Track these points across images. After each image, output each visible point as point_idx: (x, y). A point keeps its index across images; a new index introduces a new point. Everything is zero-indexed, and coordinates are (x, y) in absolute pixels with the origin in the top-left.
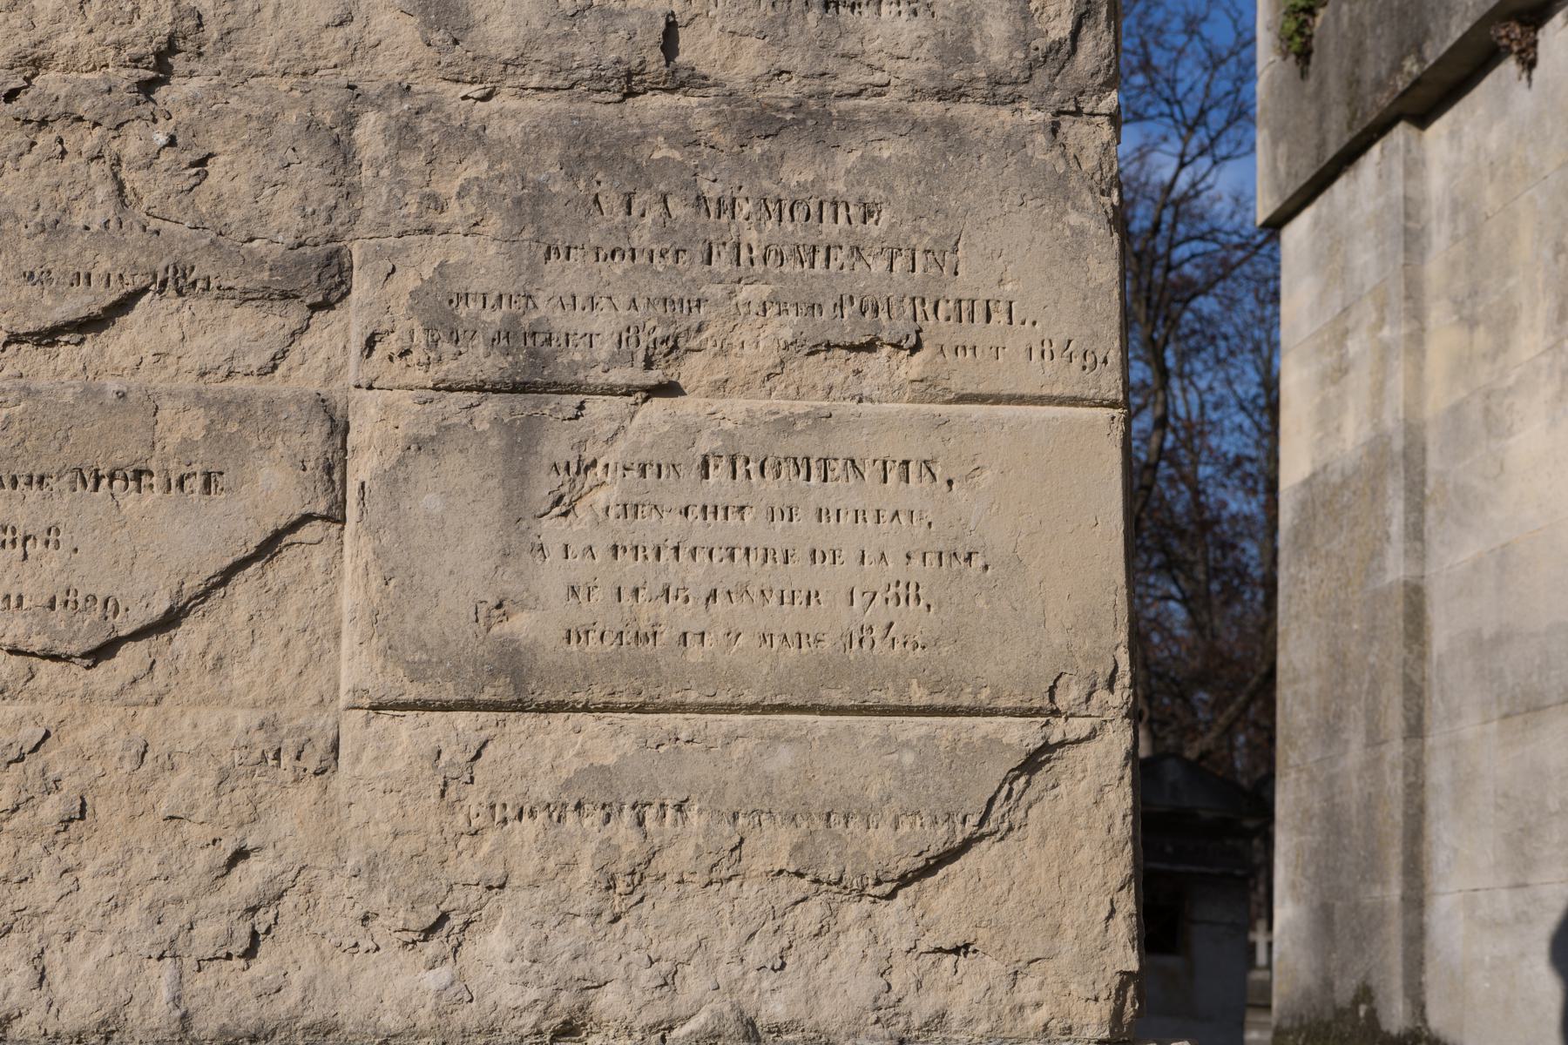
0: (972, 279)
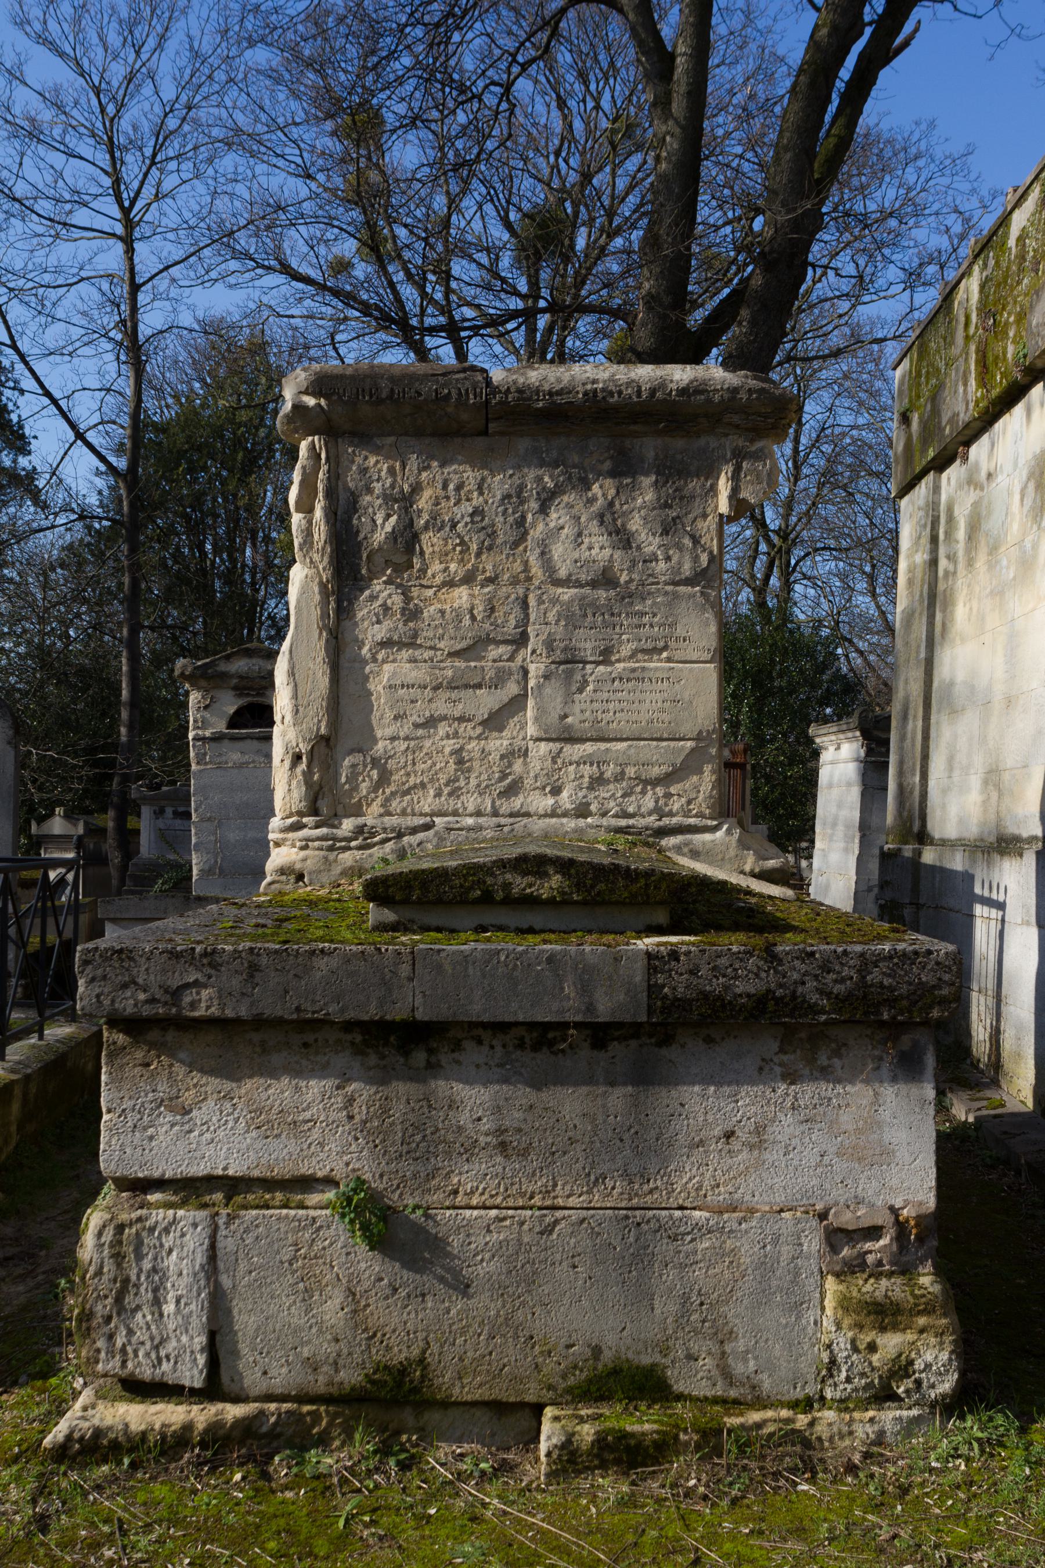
0: (680, 631)
